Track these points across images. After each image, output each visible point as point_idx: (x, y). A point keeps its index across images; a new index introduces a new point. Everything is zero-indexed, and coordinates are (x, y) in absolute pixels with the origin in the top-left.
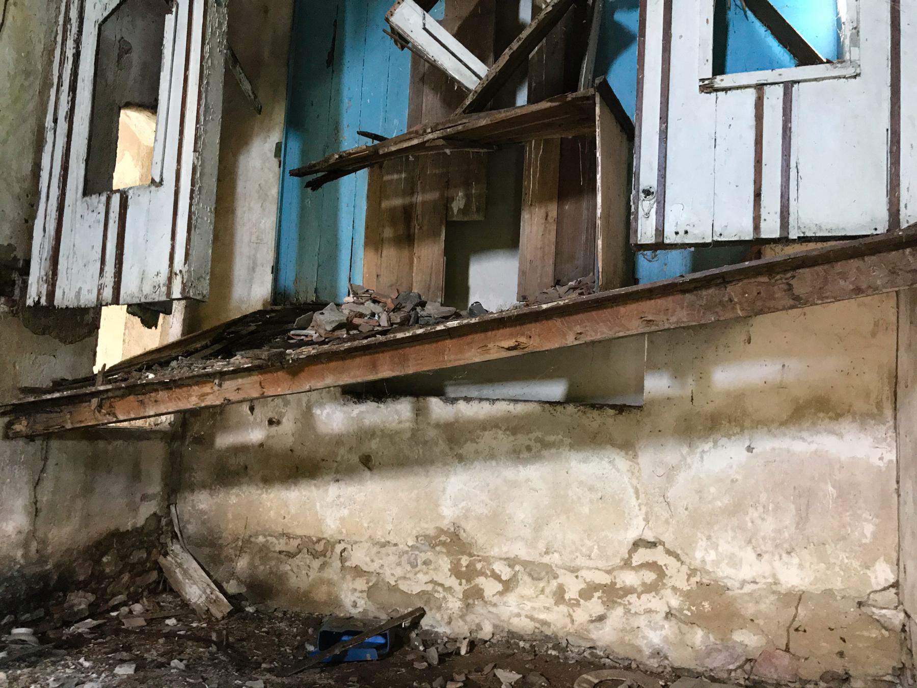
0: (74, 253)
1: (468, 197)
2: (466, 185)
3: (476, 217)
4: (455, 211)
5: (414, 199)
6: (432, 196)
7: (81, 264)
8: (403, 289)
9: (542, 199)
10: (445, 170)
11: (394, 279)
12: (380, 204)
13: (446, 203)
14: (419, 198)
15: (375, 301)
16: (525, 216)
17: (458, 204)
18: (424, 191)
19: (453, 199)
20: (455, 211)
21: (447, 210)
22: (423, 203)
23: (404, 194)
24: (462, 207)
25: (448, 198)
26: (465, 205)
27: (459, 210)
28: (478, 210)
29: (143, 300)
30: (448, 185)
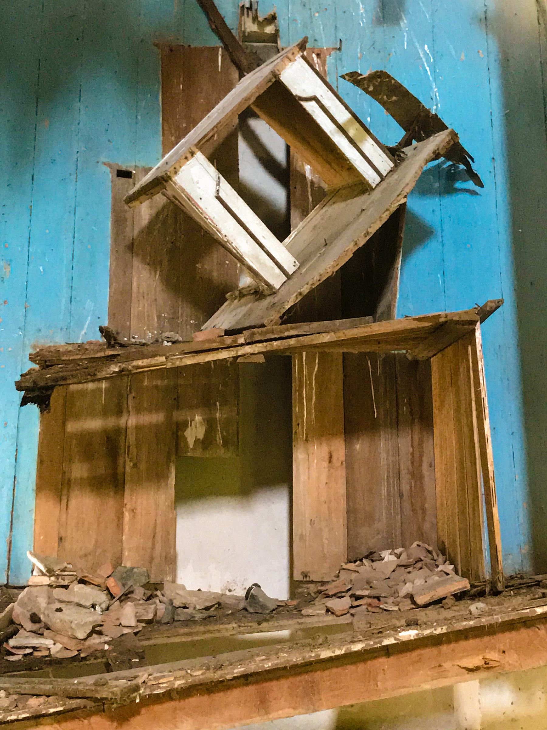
1: (210, 424)
2: (206, 403)
4: (191, 445)
9: (321, 432)
12: (64, 430)
14: (131, 421)
16: (299, 456)
20: (191, 445)
23: (105, 413)
24: (201, 436)
27: (197, 441)
28: (226, 443)
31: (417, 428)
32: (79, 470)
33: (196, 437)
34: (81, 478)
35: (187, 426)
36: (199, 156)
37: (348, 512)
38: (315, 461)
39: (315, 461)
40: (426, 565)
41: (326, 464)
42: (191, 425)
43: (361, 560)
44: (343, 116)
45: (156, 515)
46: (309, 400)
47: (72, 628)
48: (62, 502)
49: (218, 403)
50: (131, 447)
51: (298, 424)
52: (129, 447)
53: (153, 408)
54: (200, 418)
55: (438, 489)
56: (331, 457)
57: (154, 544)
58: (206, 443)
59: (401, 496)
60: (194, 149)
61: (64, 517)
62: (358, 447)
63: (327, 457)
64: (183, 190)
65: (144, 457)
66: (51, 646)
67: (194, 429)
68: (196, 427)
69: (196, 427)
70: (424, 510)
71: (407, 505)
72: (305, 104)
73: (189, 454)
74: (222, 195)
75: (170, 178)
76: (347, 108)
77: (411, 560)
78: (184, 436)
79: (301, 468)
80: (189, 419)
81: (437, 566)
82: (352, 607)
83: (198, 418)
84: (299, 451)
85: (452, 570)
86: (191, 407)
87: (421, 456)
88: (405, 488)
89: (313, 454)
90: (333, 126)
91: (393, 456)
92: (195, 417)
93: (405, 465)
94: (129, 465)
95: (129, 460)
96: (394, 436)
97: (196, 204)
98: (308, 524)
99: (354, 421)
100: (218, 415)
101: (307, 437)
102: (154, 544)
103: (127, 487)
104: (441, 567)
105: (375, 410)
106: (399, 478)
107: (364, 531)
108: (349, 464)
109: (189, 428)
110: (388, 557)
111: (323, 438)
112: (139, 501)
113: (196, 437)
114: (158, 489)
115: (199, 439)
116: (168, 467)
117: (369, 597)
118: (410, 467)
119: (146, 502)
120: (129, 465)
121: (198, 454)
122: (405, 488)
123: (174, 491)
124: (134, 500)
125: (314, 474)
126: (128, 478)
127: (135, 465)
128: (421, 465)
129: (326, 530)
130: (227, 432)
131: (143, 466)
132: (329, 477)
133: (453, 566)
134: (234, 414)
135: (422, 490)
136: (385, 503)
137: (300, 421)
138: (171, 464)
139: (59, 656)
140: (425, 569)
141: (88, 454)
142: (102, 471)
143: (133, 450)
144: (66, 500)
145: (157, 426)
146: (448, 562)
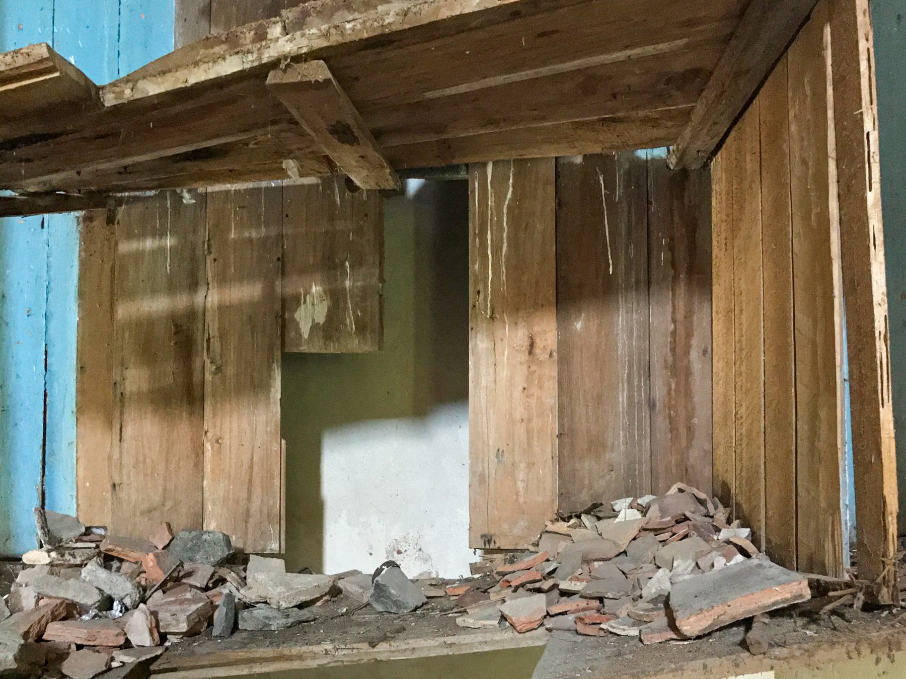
1: (335, 297)
2: (329, 266)
3: (354, 345)
4: (305, 330)
5: (199, 299)
6: (247, 292)
8: (180, 520)
10: (274, 231)
11: (157, 498)
12: (112, 318)
13: (282, 311)
14: (211, 298)
15: (107, 560)
16: (479, 345)
17: (311, 313)
18: (223, 280)
19: (296, 301)
20: (305, 330)
21: (283, 327)
22: (223, 309)
24: (321, 319)
25: (284, 301)
26: (330, 317)
27: (315, 327)
28: (361, 328)
30: (283, 268)
31: (682, 289)
32: (135, 379)
33: (313, 320)
34: (139, 393)
35: (298, 304)
37: (560, 436)
38: (506, 353)
39: (506, 353)
40: (695, 528)
41: (524, 357)
42: (305, 301)
45: (253, 447)
46: (497, 250)
48: (114, 429)
49: (347, 263)
50: (212, 340)
51: (479, 292)
52: (208, 340)
53: (242, 277)
54: (319, 289)
55: (719, 390)
56: (532, 345)
57: (250, 492)
58: (329, 329)
59: (652, 405)
62: (579, 325)
63: (527, 343)
65: (232, 356)
67: (310, 307)
68: (313, 305)
69: (313, 305)
70: (690, 429)
71: (662, 423)
73: (304, 348)
77: (669, 518)
78: (294, 320)
79: (483, 363)
80: (302, 291)
81: (718, 530)
83: (314, 289)
84: (479, 336)
85: (747, 538)
86: (305, 271)
87: (689, 335)
88: (659, 393)
89: (502, 340)
91: (639, 337)
92: (311, 287)
93: (660, 353)
94: (210, 367)
95: (209, 361)
96: (642, 304)
98: (493, 457)
99: (573, 282)
100: (348, 283)
101: (493, 312)
102: (250, 492)
104: (724, 534)
105: (610, 262)
106: (649, 376)
107: (587, 467)
108: (564, 356)
109: (303, 307)
110: (627, 514)
111: (521, 313)
112: (227, 425)
113: (313, 320)
114: (255, 405)
115: (318, 324)
116: (270, 369)
118: (670, 354)
120: (210, 367)
121: (316, 348)
122: (659, 393)
123: (279, 408)
124: (218, 423)
125: (504, 373)
126: (208, 389)
127: (219, 369)
128: (687, 352)
129: (523, 465)
130: (364, 311)
131: (230, 370)
132: (531, 374)
133: (749, 530)
134: (375, 280)
135: (688, 394)
136: (623, 420)
137: (481, 287)
138: (275, 366)
140: (695, 538)
141: (148, 354)
142: (170, 380)
143: (216, 344)
144: (118, 426)
145: (252, 304)
146: (736, 522)
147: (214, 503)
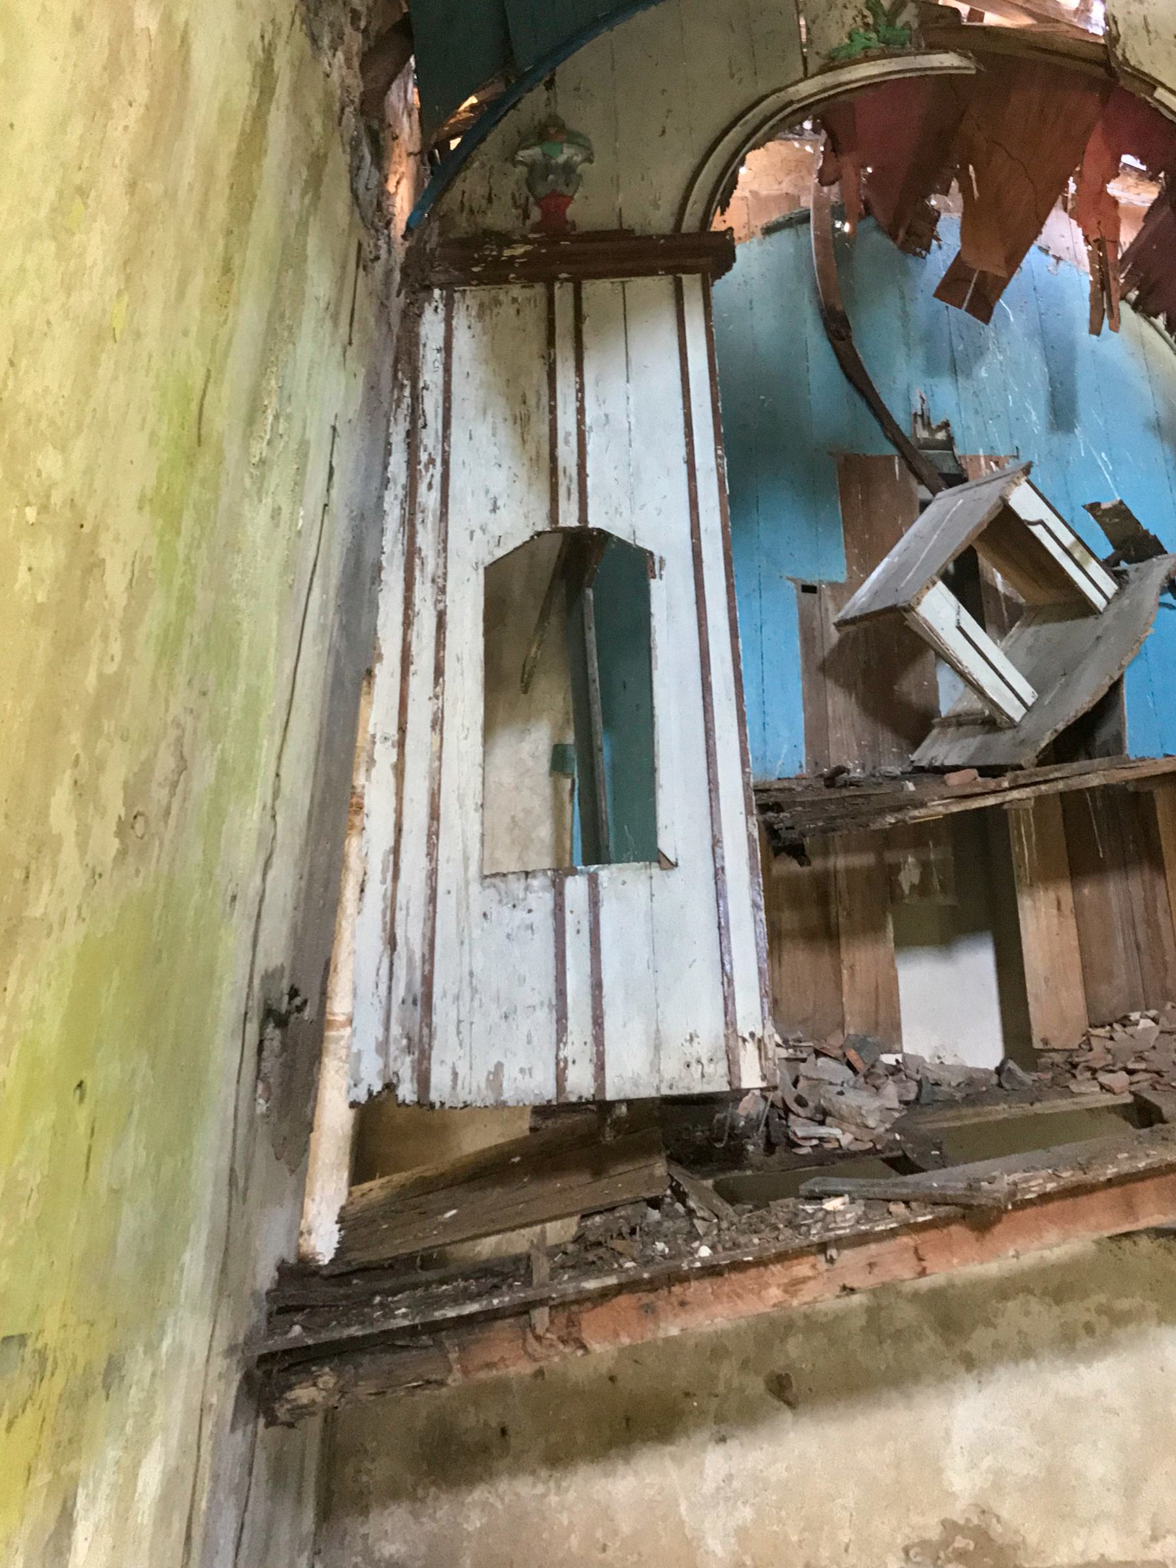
0: (474, 991)
7: (495, 1013)
19: (896, 869)
29: (665, 1091)
36: (940, 585)
43: (1111, 1025)
44: (1068, 539)
47: (861, 1115)
60: (935, 578)
61: (776, 974)
64: (926, 622)
66: (840, 1136)
72: (1033, 529)
74: (963, 625)
75: (913, 609)
76: (1071, 531)
82: (1131, 1084)
90: (1060, 550)
97: (937, 636)
103: (843, 940)
117: (1146, 1071)
119: (860, 959)
139: (854, 1147)
147: (852, 1015)
